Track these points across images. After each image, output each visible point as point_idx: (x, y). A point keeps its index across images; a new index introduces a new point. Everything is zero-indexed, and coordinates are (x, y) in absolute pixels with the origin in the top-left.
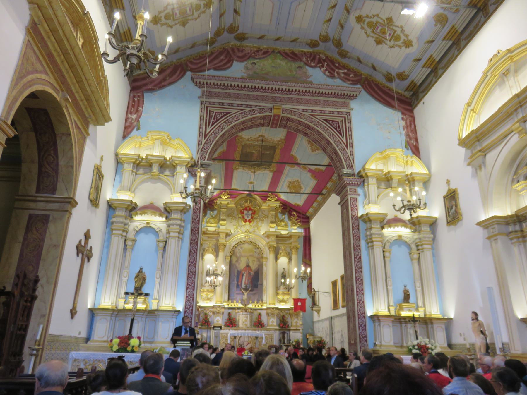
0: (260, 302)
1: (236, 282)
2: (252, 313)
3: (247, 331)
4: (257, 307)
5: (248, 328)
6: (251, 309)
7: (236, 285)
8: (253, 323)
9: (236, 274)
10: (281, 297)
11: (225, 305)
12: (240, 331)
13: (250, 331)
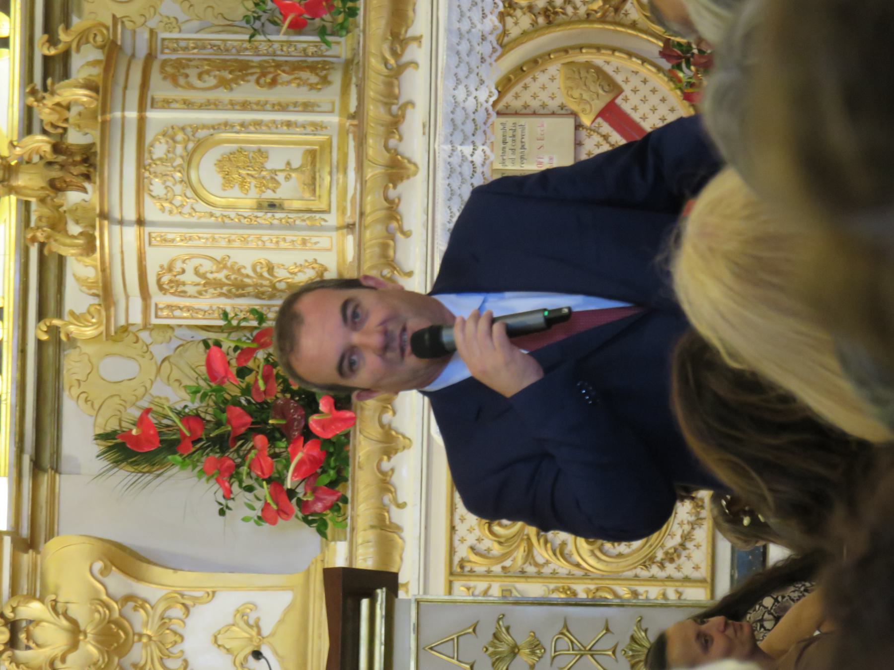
3: (414, 144)
13: (415, 85)
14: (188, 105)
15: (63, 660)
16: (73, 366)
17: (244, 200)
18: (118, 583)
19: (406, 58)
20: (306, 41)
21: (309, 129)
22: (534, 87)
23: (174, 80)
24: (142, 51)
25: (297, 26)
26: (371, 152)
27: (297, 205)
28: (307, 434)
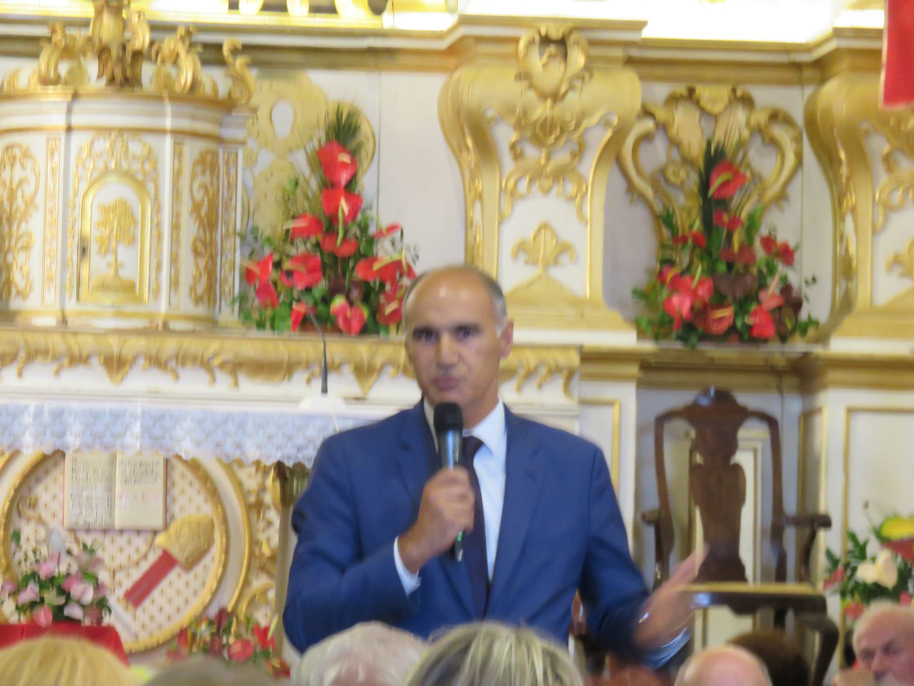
3: (140, 381)
8: (235, 259)
12: (39, 378)
13: (193, 383)
14: (177, 175)
17: (90, 224)
19: (219, 375)
20: (235, 283)
21: (153, 286)
24: (228, 133)
25: (248, 276)
27: (85, 273)
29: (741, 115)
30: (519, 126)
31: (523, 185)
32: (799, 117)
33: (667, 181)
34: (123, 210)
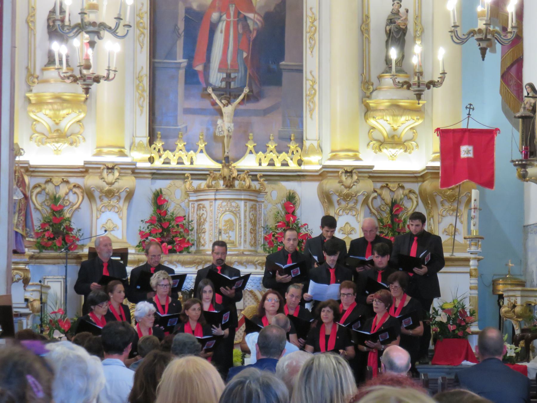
0: (293, 146)
1: (182, 61)
2: (255, 196)
4: (278, 166)
5: (243, 254)
6: (253, 175)
7: (182, 73)
8: (262, 234)
9: (181, 25)
10: (383, 124)
11: (139, 158)
14: (245, 211)
15: (104, 181)
16: (179, 183)
17: (221, 226)
18: (123, 195)
19: (258, 266)
22: (251, 299)
23: (252, 208)
24: (258, 199)
25: (265, 238)
26: (234, 258)
28: (162, 242)
29: (401, 191)
30: (339, 196)
31: (341, 213)
32: (417, 192)
33: (381, 210)
34: (229, 221)
